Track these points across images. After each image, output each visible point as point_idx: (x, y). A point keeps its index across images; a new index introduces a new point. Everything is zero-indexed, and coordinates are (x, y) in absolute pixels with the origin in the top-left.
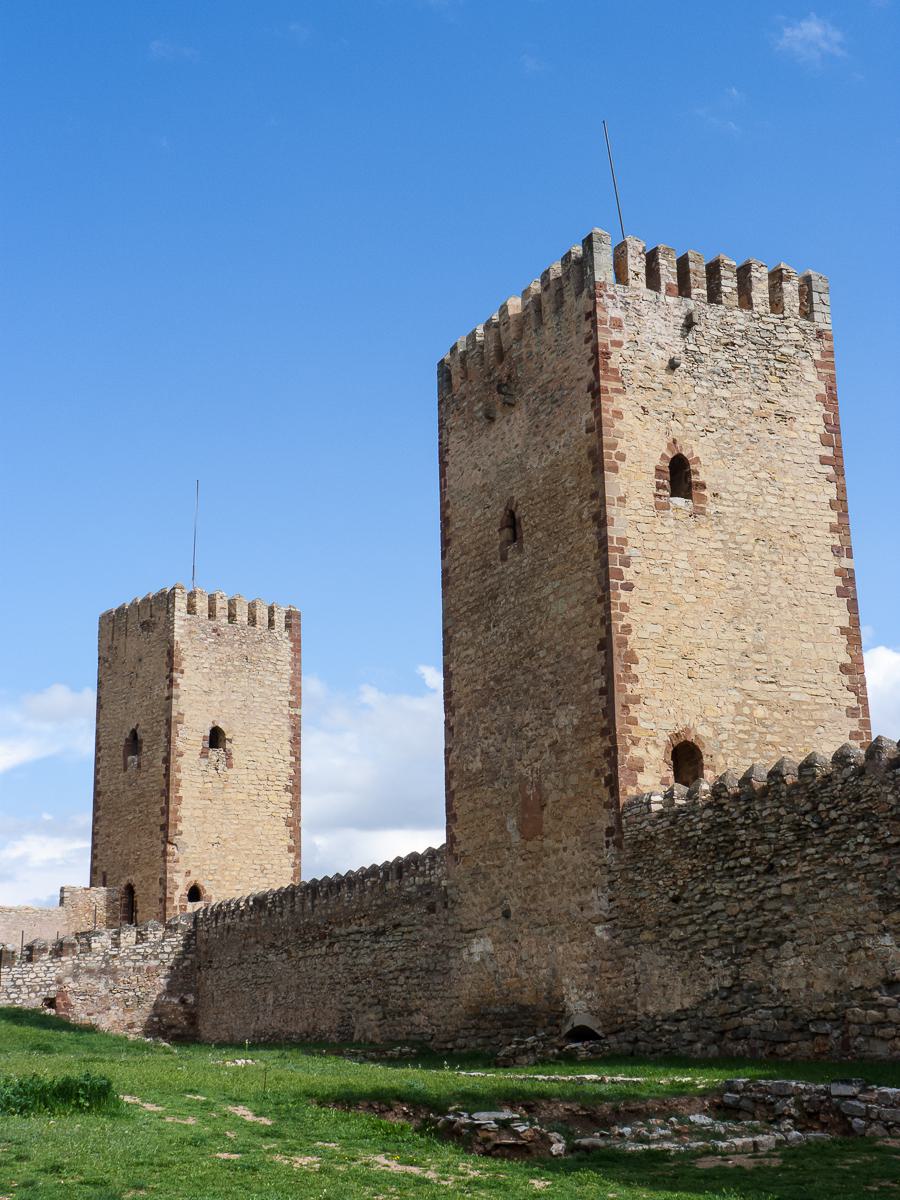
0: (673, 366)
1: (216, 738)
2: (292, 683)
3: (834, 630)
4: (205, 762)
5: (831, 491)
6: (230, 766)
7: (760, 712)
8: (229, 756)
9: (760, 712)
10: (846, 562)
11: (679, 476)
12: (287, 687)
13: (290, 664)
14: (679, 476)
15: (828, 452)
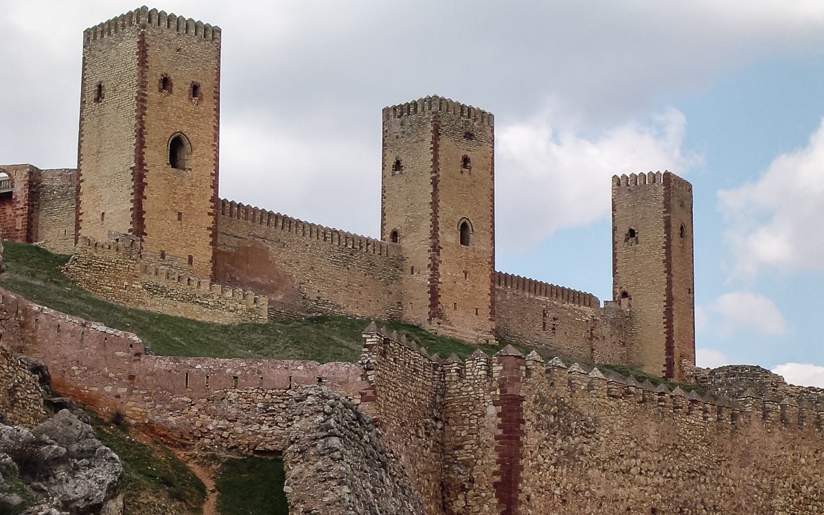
0: (397, 137)
1: (632, 233)
2: (665, 203)
3: (429, 194)
4: (626, 243)
5: (432, 156)
6: (637, 243)
7: (411, 220)
8: (637, 239)
9: (411, 220)
10: (434, 175)
11: (398, 166)
12: (662, 206)
13: (663, 195)
14: (398, 166)
15: (432, 146)
